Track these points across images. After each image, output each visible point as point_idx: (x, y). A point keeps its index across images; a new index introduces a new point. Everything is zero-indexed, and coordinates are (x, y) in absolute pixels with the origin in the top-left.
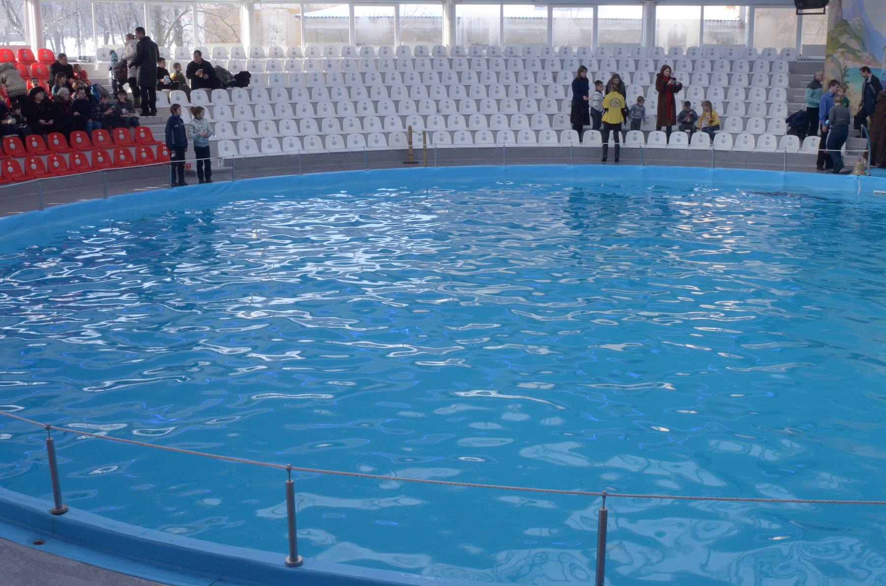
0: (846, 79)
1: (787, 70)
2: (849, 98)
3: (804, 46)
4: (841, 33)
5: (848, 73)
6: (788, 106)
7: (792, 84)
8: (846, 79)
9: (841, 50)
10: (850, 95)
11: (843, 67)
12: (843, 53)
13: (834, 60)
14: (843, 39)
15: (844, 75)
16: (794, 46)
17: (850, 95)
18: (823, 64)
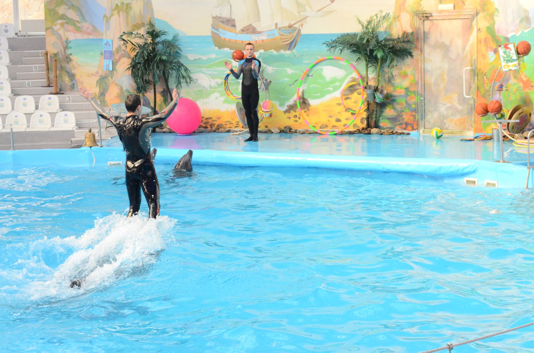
0: (69, 52)
1: (7, 47)
2: (73, 71)
3: (22, 21)
4: (59, 4)
5: (70, 45)
6: (11, 83)
7: (13, 61)
8: (69, 52)
9: (60, 21)
10: (74, 68)
11: (64, 39)
12: (62, 25)
13: (54, 33)
14: (61, 10)
15: (66, 48)
16: (11, 21)
17: (74, 68)
18: (45, 39)
